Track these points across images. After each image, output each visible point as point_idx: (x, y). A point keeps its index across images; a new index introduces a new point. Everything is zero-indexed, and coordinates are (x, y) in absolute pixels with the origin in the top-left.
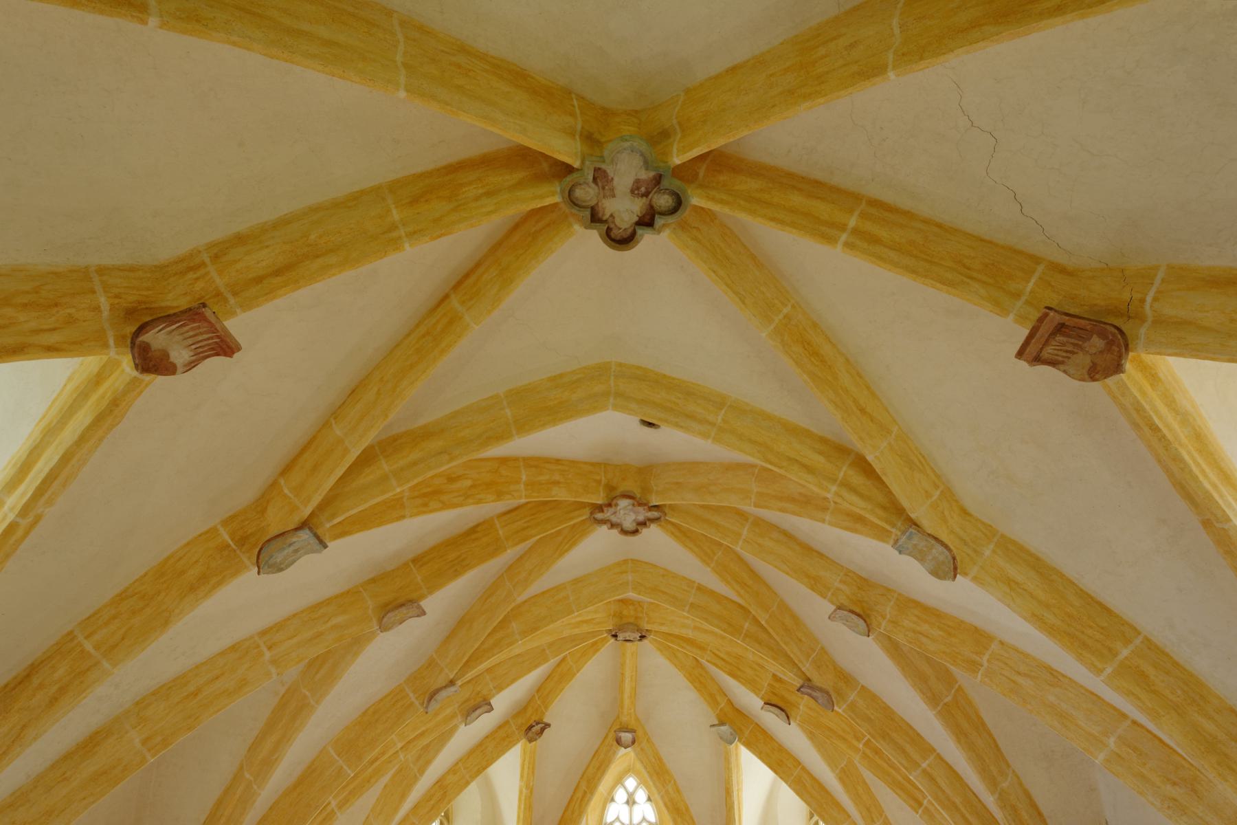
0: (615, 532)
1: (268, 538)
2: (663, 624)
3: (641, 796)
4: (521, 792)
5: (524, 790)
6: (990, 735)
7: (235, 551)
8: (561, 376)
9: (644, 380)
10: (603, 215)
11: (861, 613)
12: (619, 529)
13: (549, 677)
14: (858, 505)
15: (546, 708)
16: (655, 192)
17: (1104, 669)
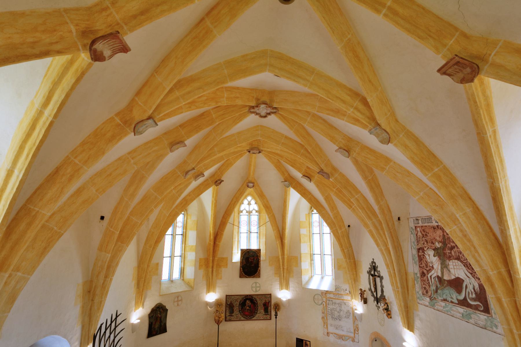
0: (257, 116)
1: (135, 123)
2: (268, 148)
3: (253, 202)
4: (213, 202)
5: (214, 201)
6: (381, 188)
7: (123, 126)
8: (247, 55)
9: (282, 59)
11: (347, 150)
12: (259, 115)
13: (223, 165)
14: (359, 115)
15: (222, 175)
17: (428, 174)
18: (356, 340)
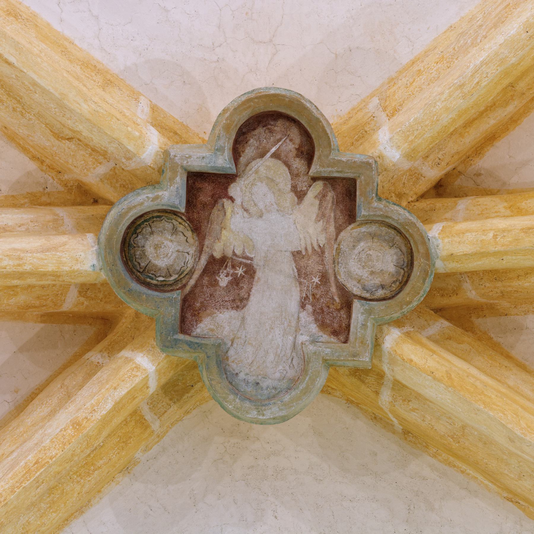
10: (322, 197)
16: (191, 272)
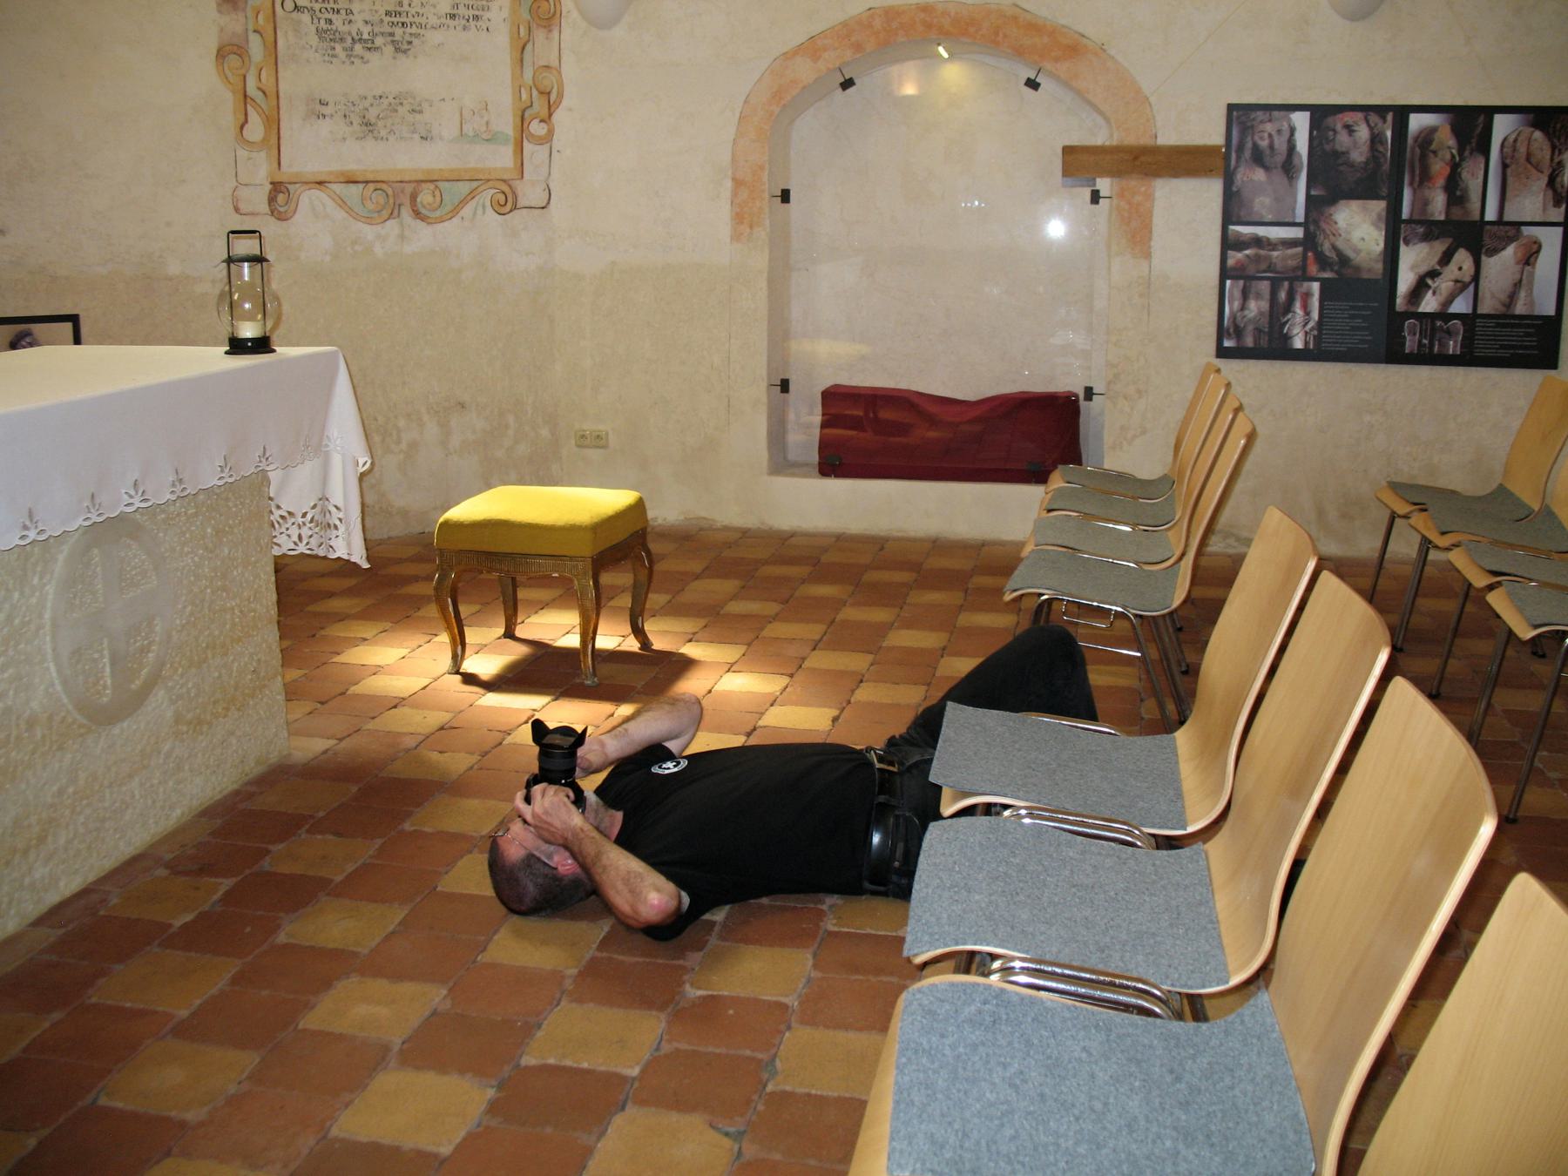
18: (530, 193)
